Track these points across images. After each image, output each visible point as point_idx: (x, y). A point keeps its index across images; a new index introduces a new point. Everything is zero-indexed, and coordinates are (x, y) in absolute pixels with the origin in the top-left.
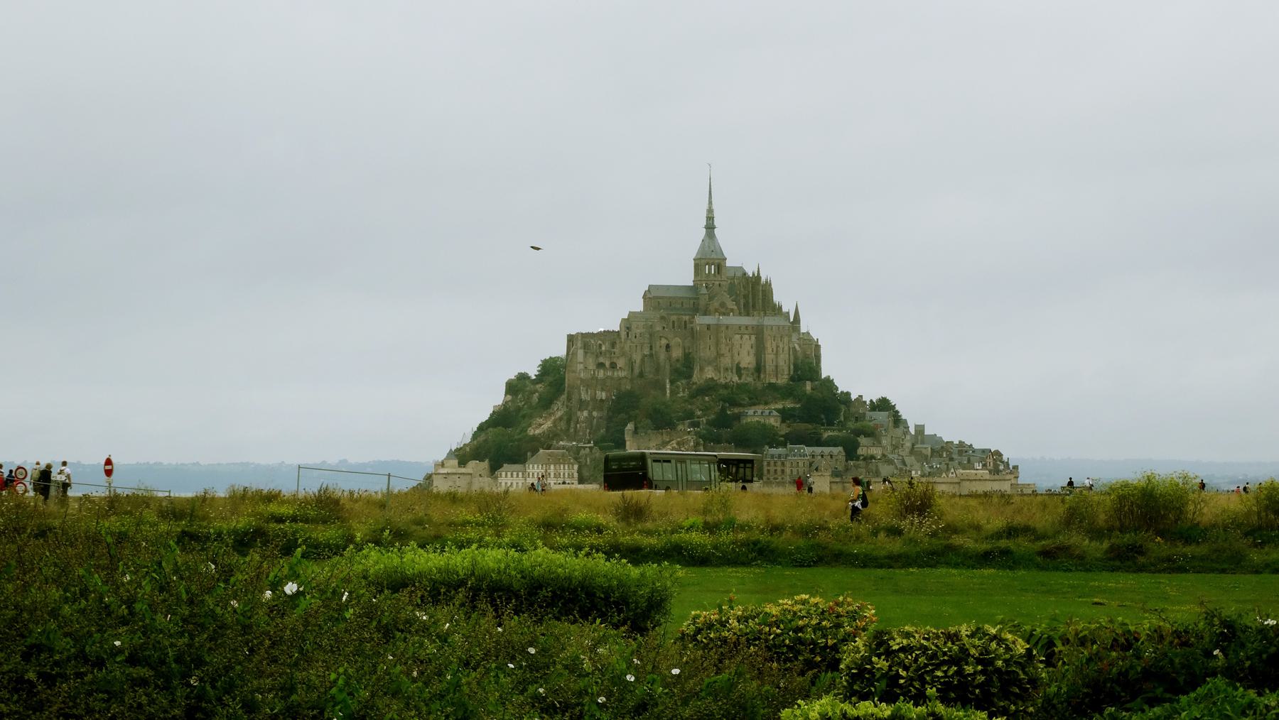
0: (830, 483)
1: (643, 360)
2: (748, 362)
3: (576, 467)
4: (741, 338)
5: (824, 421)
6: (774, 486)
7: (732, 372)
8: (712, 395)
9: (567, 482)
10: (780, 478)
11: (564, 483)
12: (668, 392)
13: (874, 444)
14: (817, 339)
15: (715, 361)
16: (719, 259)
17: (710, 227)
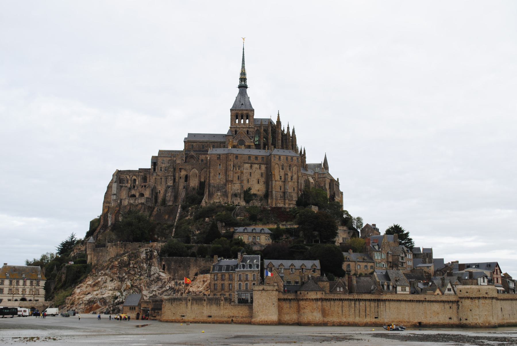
0: (279, 300)
1: (166, 191)
2: (257, 189)
3: (42, 283)
4: (251, 167)
5: (318, 238)
6: (205, 303)
7: (240, 197)
8: (213, 217)
9: (28, 299)
10: (227, 294)
11: (23, 299)
12: (178, 215)
13: (364, 259)
14: (338, 179)
15: (222, 189)
16: (247, 110)
17: (243, 87)
